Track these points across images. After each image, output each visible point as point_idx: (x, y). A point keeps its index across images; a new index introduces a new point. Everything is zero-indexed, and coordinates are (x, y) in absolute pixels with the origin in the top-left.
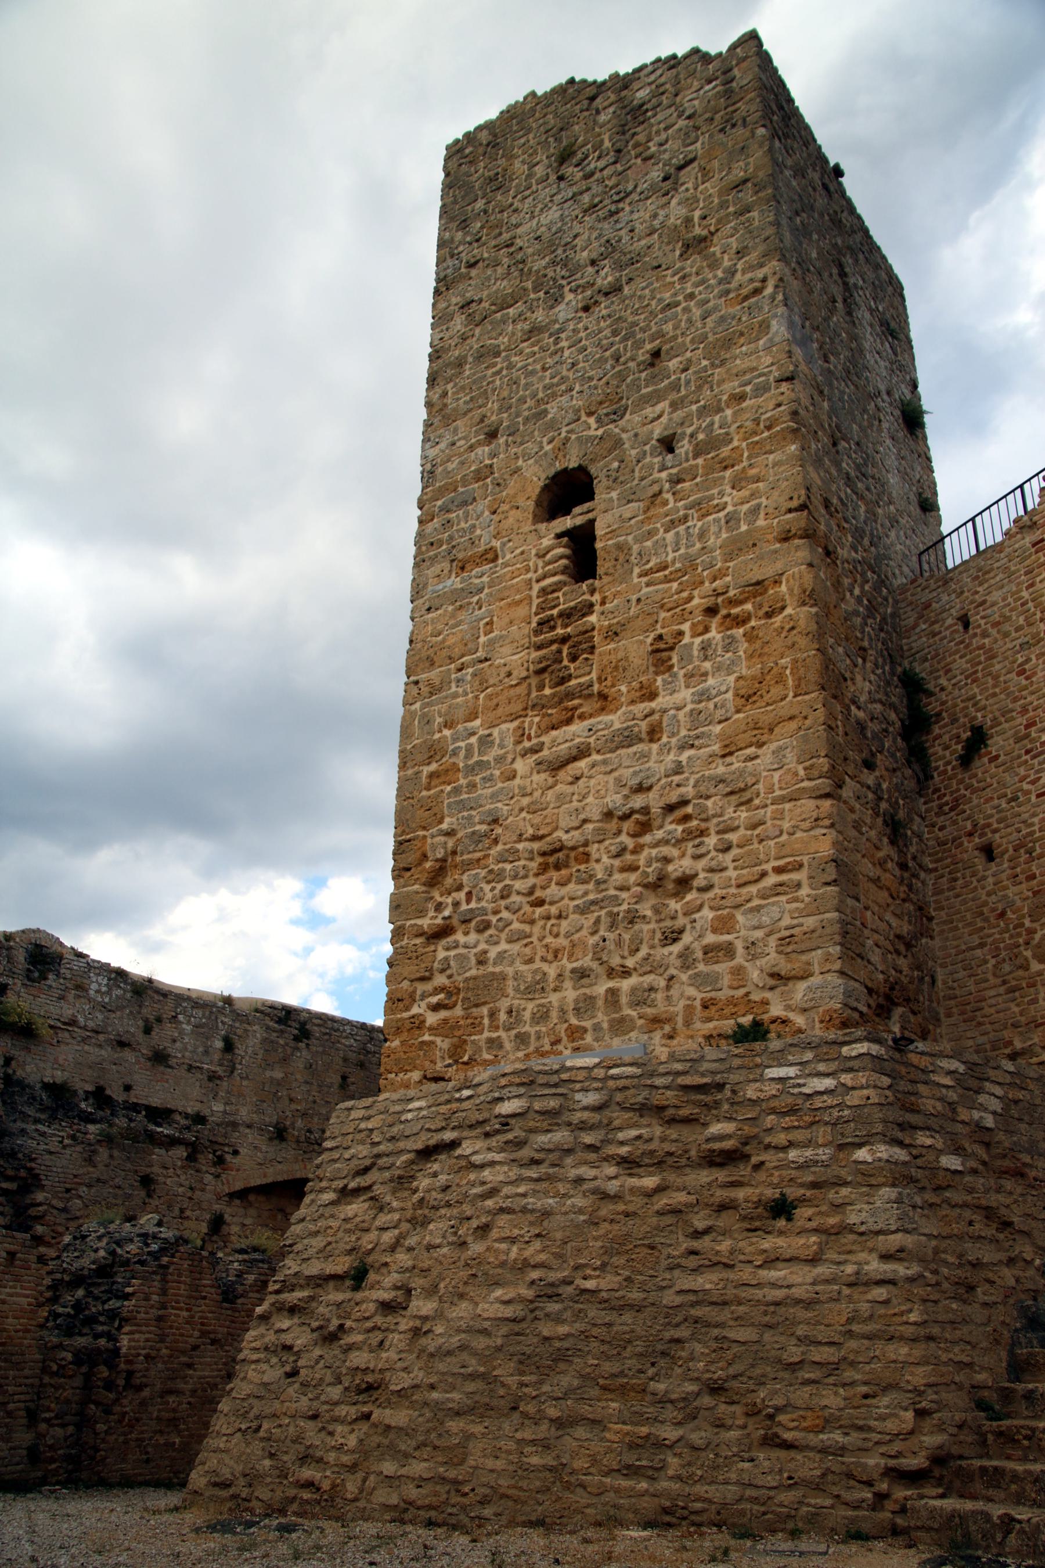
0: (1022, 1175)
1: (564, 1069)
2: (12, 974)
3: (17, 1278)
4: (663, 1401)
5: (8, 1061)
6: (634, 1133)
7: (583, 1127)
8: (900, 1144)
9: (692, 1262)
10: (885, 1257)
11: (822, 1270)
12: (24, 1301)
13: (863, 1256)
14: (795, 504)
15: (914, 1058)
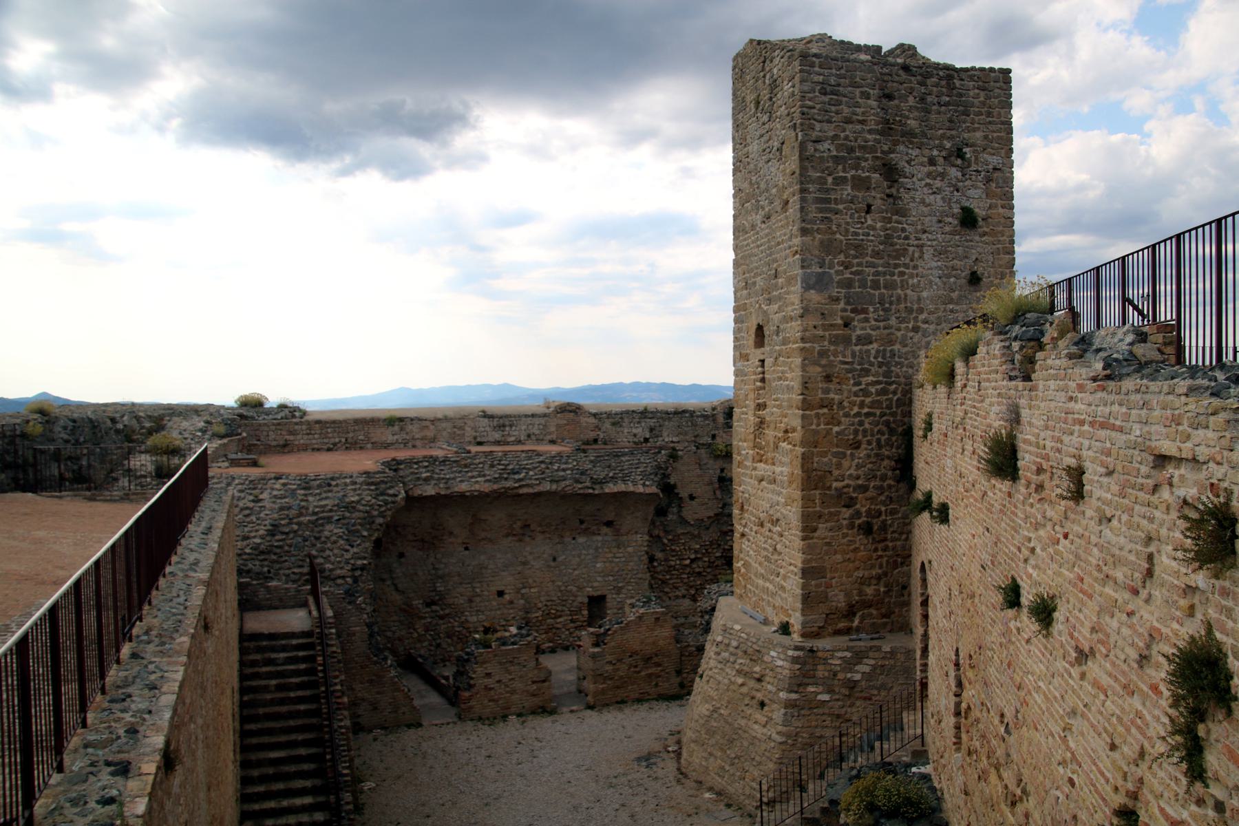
0: (870, 699)
1: (732, 629)
2: (717, 428)
3: (662, 626)
4: (728, 756)
5: (722, 470)
6: (741, 661)
7: (732, 654)
8: (796, 692)
9: (742, 714)
10: (778, 733)
11: (765, 730)
12: (667, 634)
13: (773, 730)
14: (799, 392)
15: (820, 654)
